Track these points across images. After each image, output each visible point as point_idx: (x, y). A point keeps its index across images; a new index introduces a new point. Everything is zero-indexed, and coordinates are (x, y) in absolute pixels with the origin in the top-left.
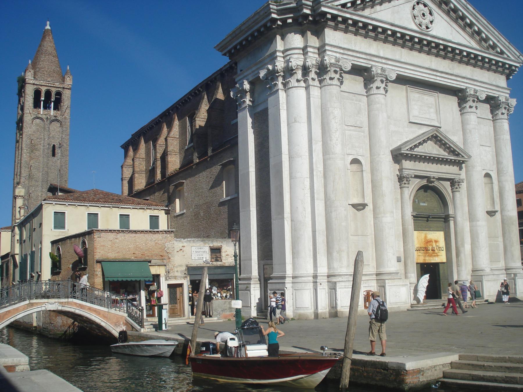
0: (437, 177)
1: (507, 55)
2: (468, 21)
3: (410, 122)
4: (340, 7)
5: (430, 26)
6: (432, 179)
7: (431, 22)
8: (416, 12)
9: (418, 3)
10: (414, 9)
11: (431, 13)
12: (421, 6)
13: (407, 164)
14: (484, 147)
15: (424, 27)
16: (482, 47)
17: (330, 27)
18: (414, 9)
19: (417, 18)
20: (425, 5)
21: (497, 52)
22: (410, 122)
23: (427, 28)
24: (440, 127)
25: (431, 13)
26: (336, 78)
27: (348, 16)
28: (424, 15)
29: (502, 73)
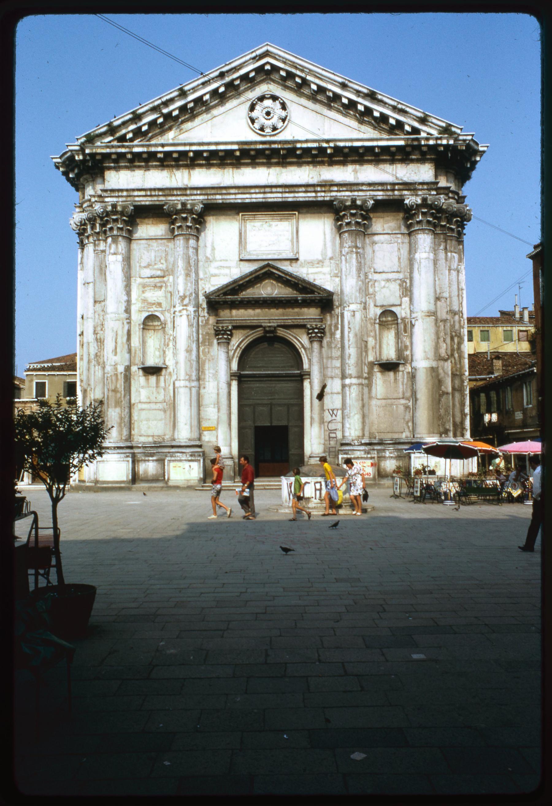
0: (275, 325)
1: (424, 131)
2: (345, 101)
3: (241, 260)
4: (115, 143)
5: (280, 124)
6: (268, 329)
7: (284, 120)
8: (254, 114)
9: (262, 99)
10: (252, 108)
11: (284, 107)
12: (268, 103)
13: (225, 314)
14: (384, 275)
15: (268, 130)
16: (382, 130)
17: (109, 168)
18: (252, 108)
19: (256, 121)
20: (274, 98)
21: (407, 132)
22: (241, 260)
23: (274, 129)
24: (297, 259)
25: (284, 107)
26: (115, 228)
27: (123, 150)
28: (268, 114)
29: (422, 160)
